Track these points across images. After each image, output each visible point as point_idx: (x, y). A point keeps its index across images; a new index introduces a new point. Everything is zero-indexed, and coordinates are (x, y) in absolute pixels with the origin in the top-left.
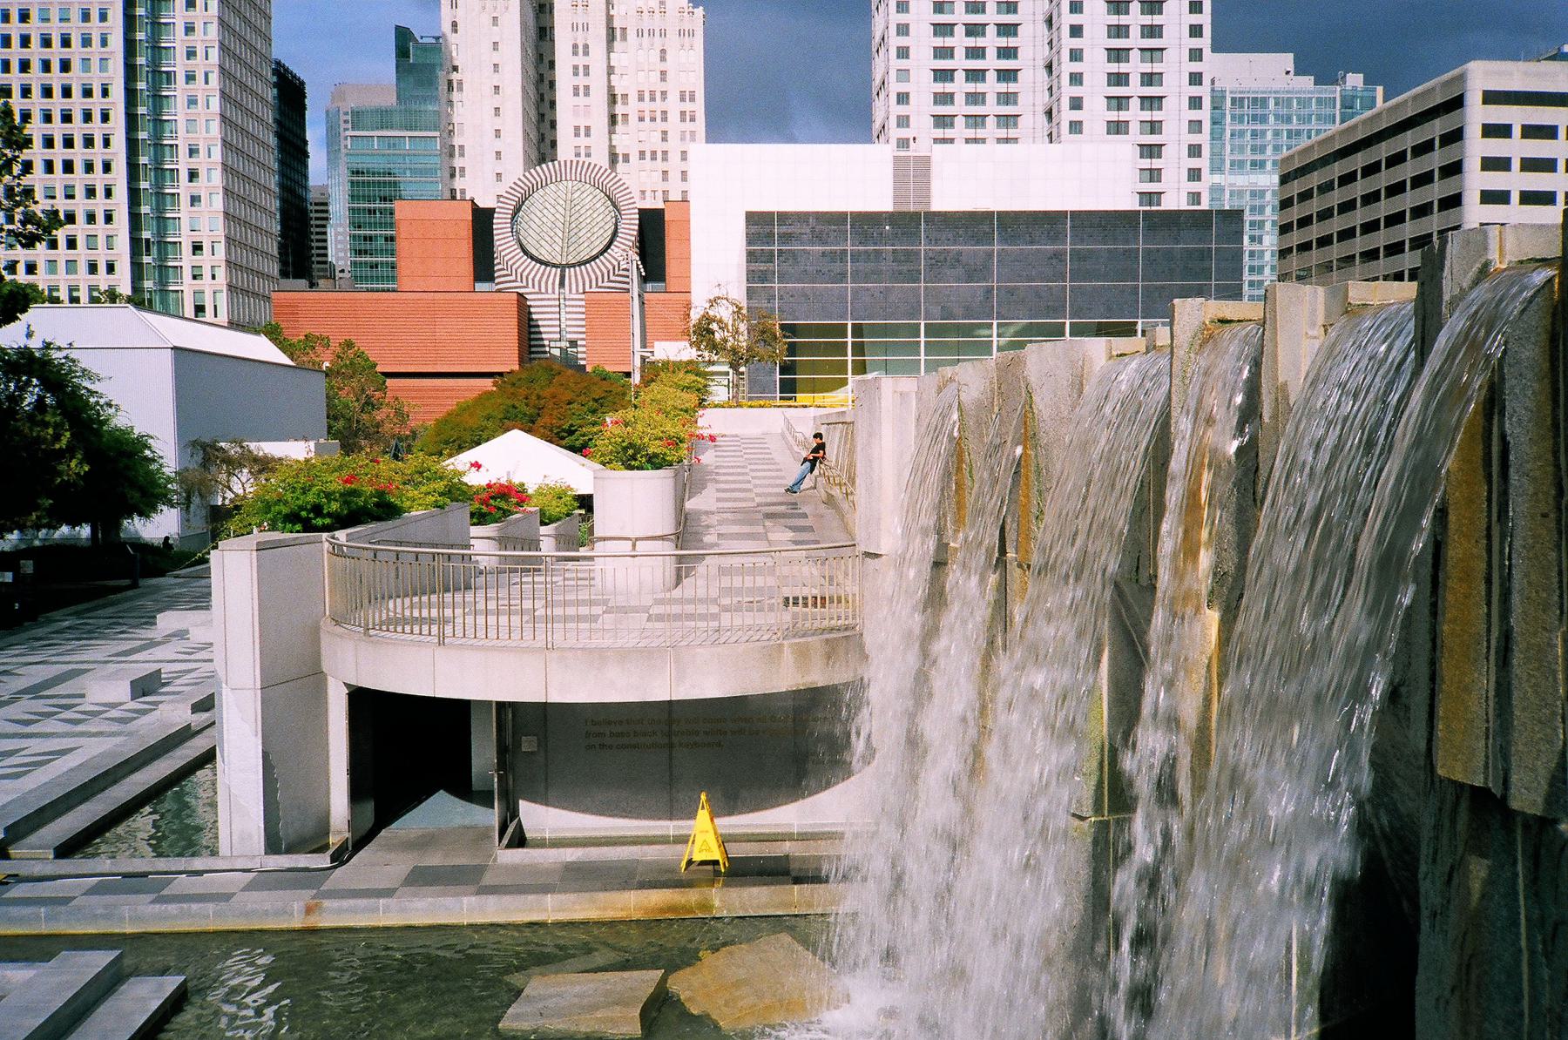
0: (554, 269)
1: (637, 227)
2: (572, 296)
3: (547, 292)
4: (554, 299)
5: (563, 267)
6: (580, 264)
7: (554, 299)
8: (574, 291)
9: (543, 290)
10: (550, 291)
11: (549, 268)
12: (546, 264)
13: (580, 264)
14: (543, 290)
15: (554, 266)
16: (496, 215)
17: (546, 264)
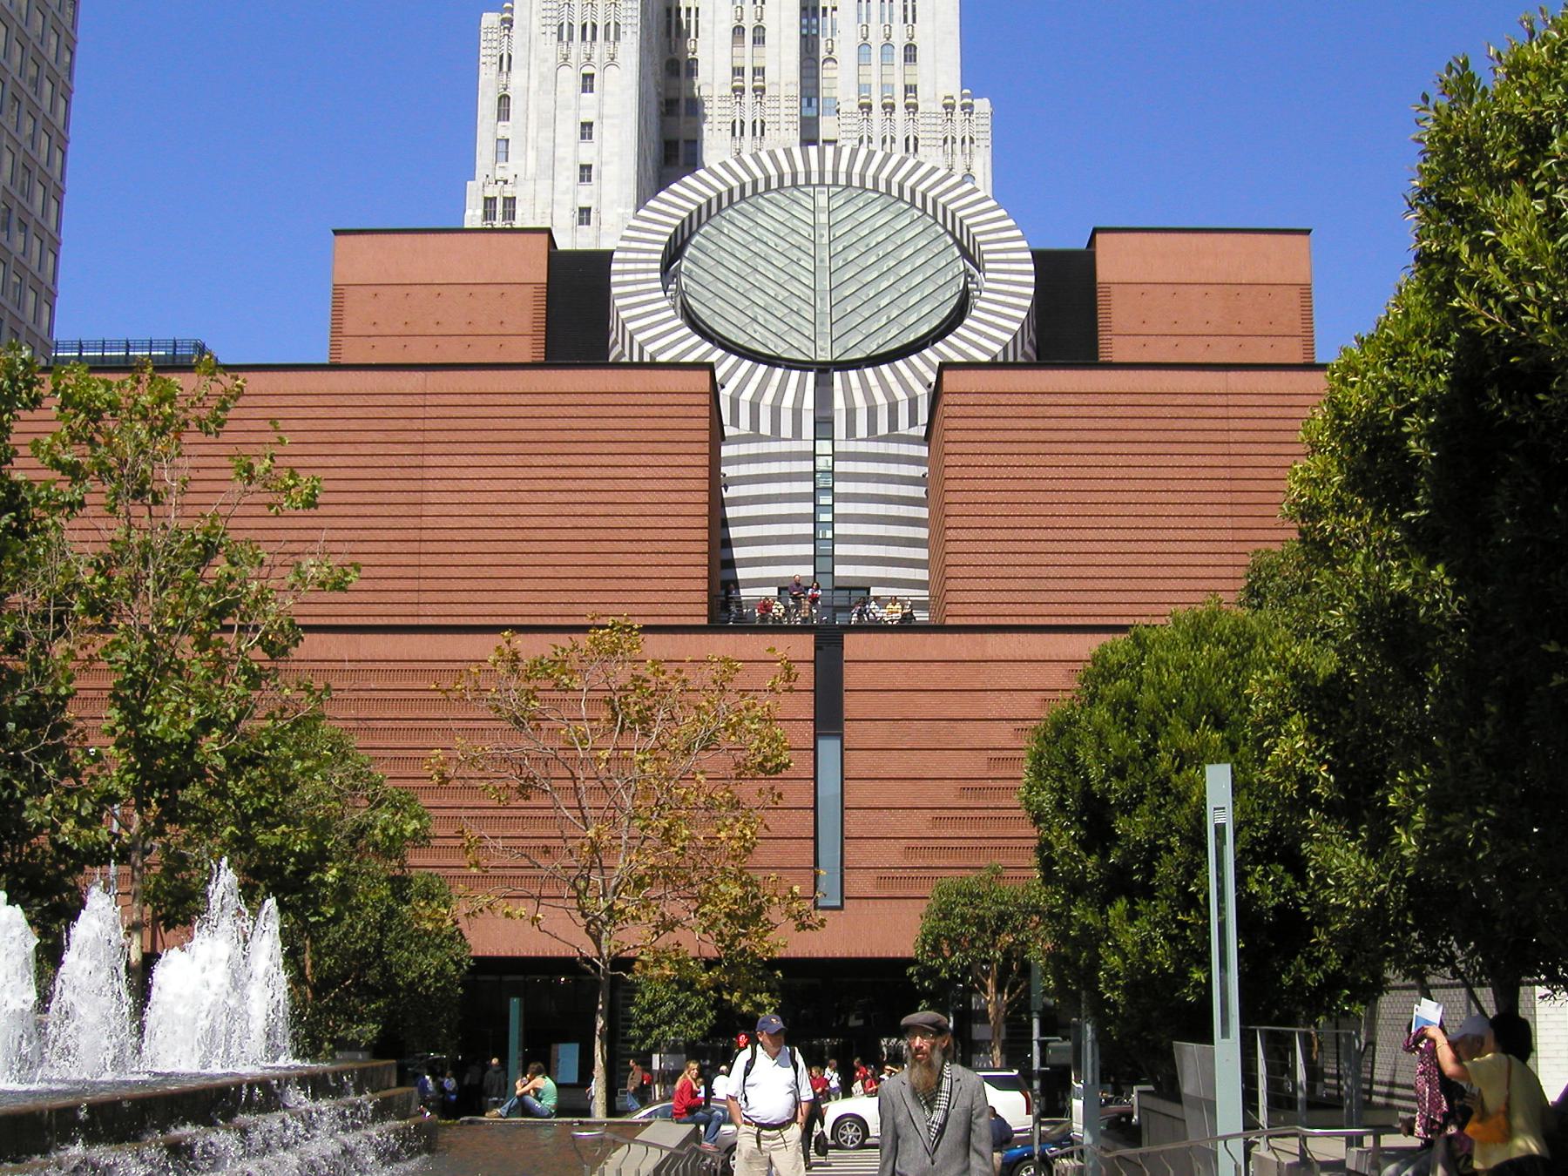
0: (795, 374)
1: (1032, 279)
2: (852, 447)
3: (776, 435)
4: (800, 456)
5: (824, 370)
6: (874, 361)
7: (800, 456)
8: (862, 429)
9: (765, 428)
10: (786, 429)
11: (779, 372)
12: (773, 361)
13: (874, 361)
14: (765, 428)
15: (791, 365)
16: (614, 267)
17: (773, 361)
